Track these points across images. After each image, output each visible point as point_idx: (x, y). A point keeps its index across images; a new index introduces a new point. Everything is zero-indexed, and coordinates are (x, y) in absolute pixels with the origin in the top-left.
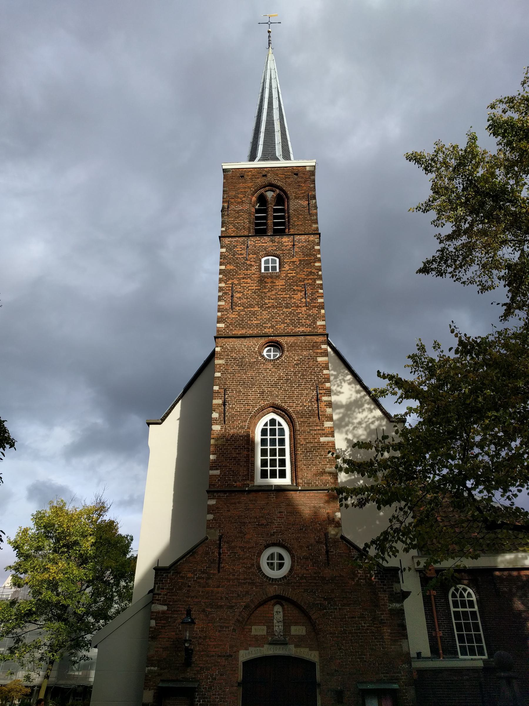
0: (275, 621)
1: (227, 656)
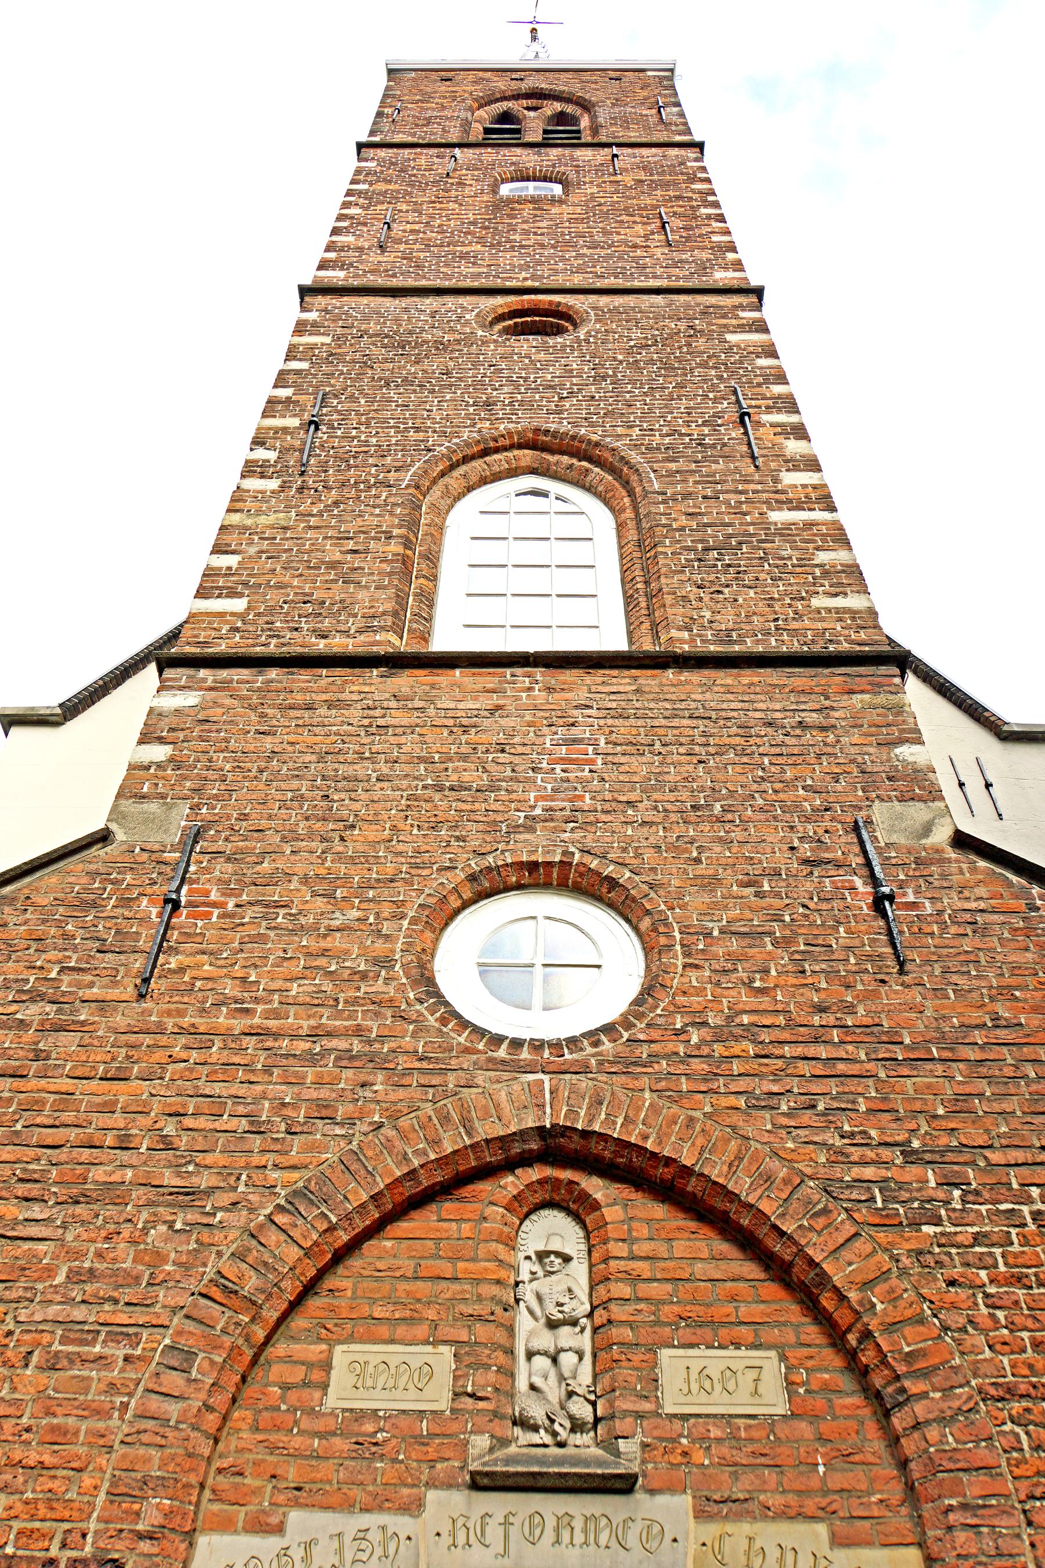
0: (523, 1322)
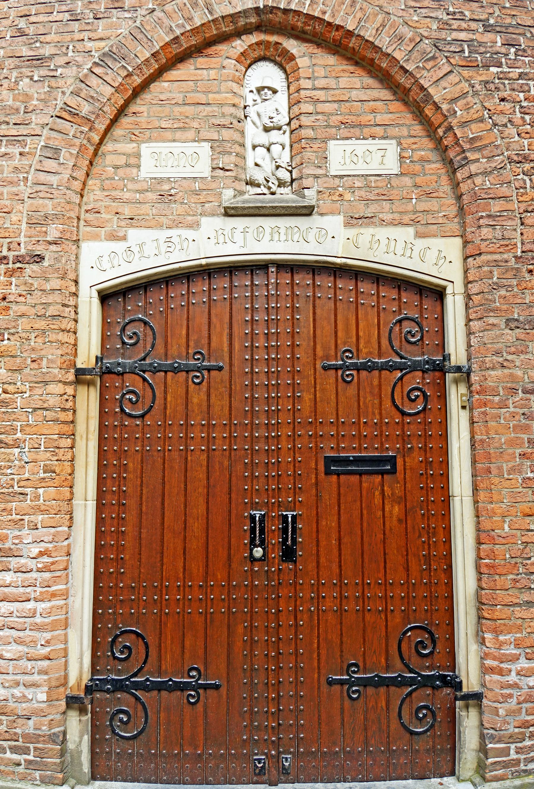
1: (18, 259)
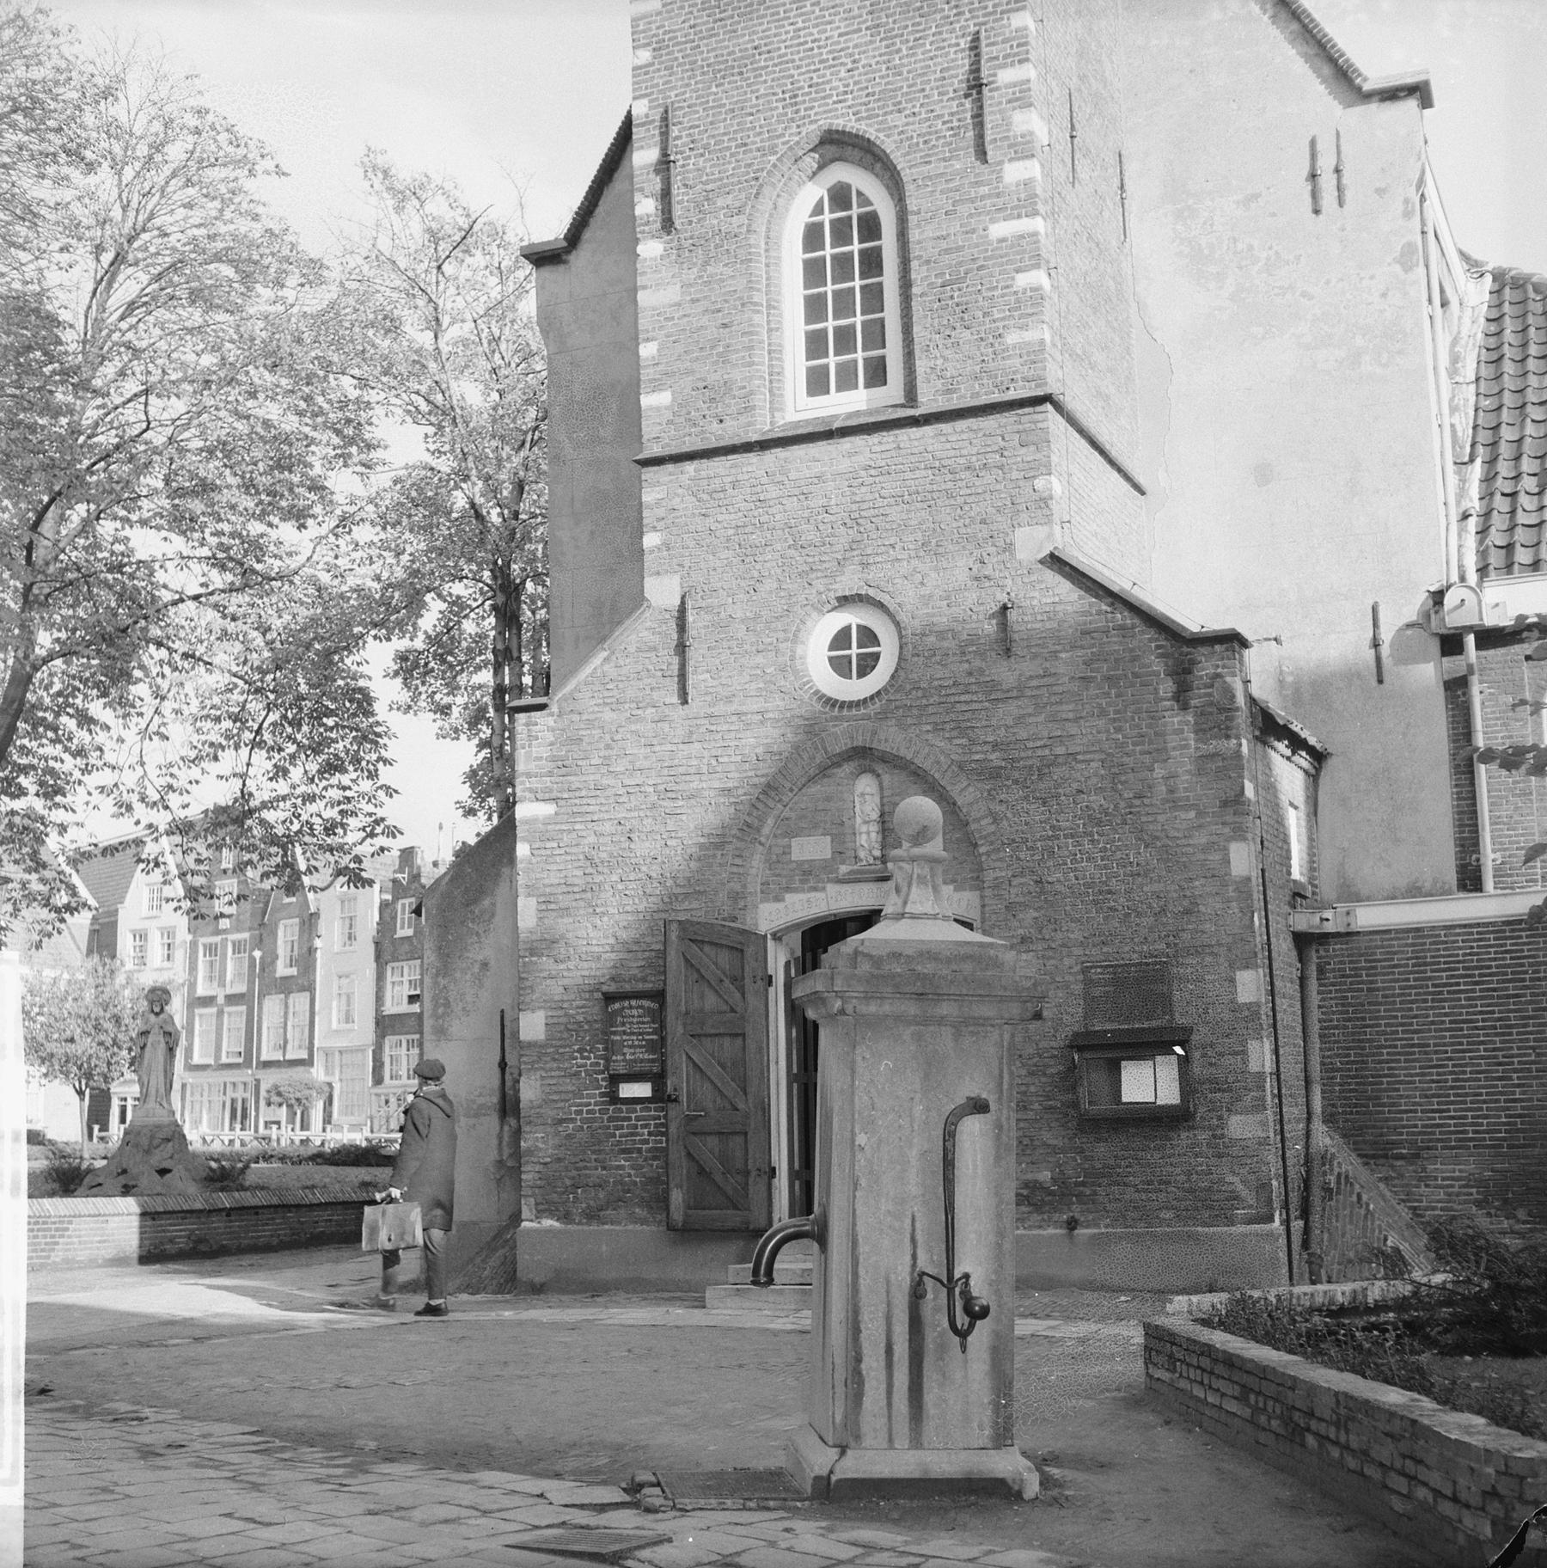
0: (859, 820)
